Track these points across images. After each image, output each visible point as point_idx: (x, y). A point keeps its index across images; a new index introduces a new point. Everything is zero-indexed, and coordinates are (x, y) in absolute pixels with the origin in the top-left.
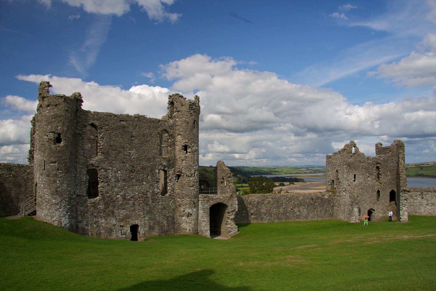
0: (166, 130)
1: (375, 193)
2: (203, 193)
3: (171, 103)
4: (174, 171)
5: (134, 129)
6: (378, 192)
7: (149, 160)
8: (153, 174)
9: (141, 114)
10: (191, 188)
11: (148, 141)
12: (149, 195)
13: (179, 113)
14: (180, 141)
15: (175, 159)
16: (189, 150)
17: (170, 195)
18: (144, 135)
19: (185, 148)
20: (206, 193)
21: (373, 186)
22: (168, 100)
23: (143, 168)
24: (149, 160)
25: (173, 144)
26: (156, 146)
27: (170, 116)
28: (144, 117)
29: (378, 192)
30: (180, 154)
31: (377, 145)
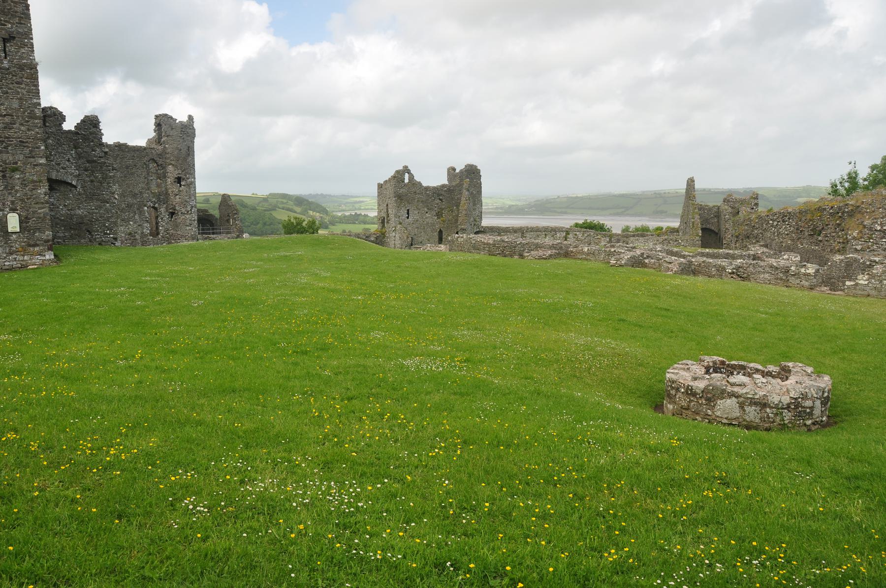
0: (153, 159)
1: (436, 234)
2: (203, 233)
3: (158, 125)
4: (166, 208)
5: (115, 160)
6: (441, 232)
7: (134, 196)
8: (141, 212)
9: (122, 142)
10: (188, 228)
11: (132, 174)
12: (138, 237)
13: (170, 138)
14: (172, 172)
15: (167, 194)
16: (183, 183)
17: (163, 237)
18: (127, 167)
19: (179, 180)
20: (206, 234)
21: (433, 225)
22: (154, 121)
23: (130, 206)
24: (134, 196)
25: (163, 177)
26: (142, 179)
27: (158, 140)
28: (125, 145)
29: (441, 232)
30: (173, 189)
31: (448, 170)
